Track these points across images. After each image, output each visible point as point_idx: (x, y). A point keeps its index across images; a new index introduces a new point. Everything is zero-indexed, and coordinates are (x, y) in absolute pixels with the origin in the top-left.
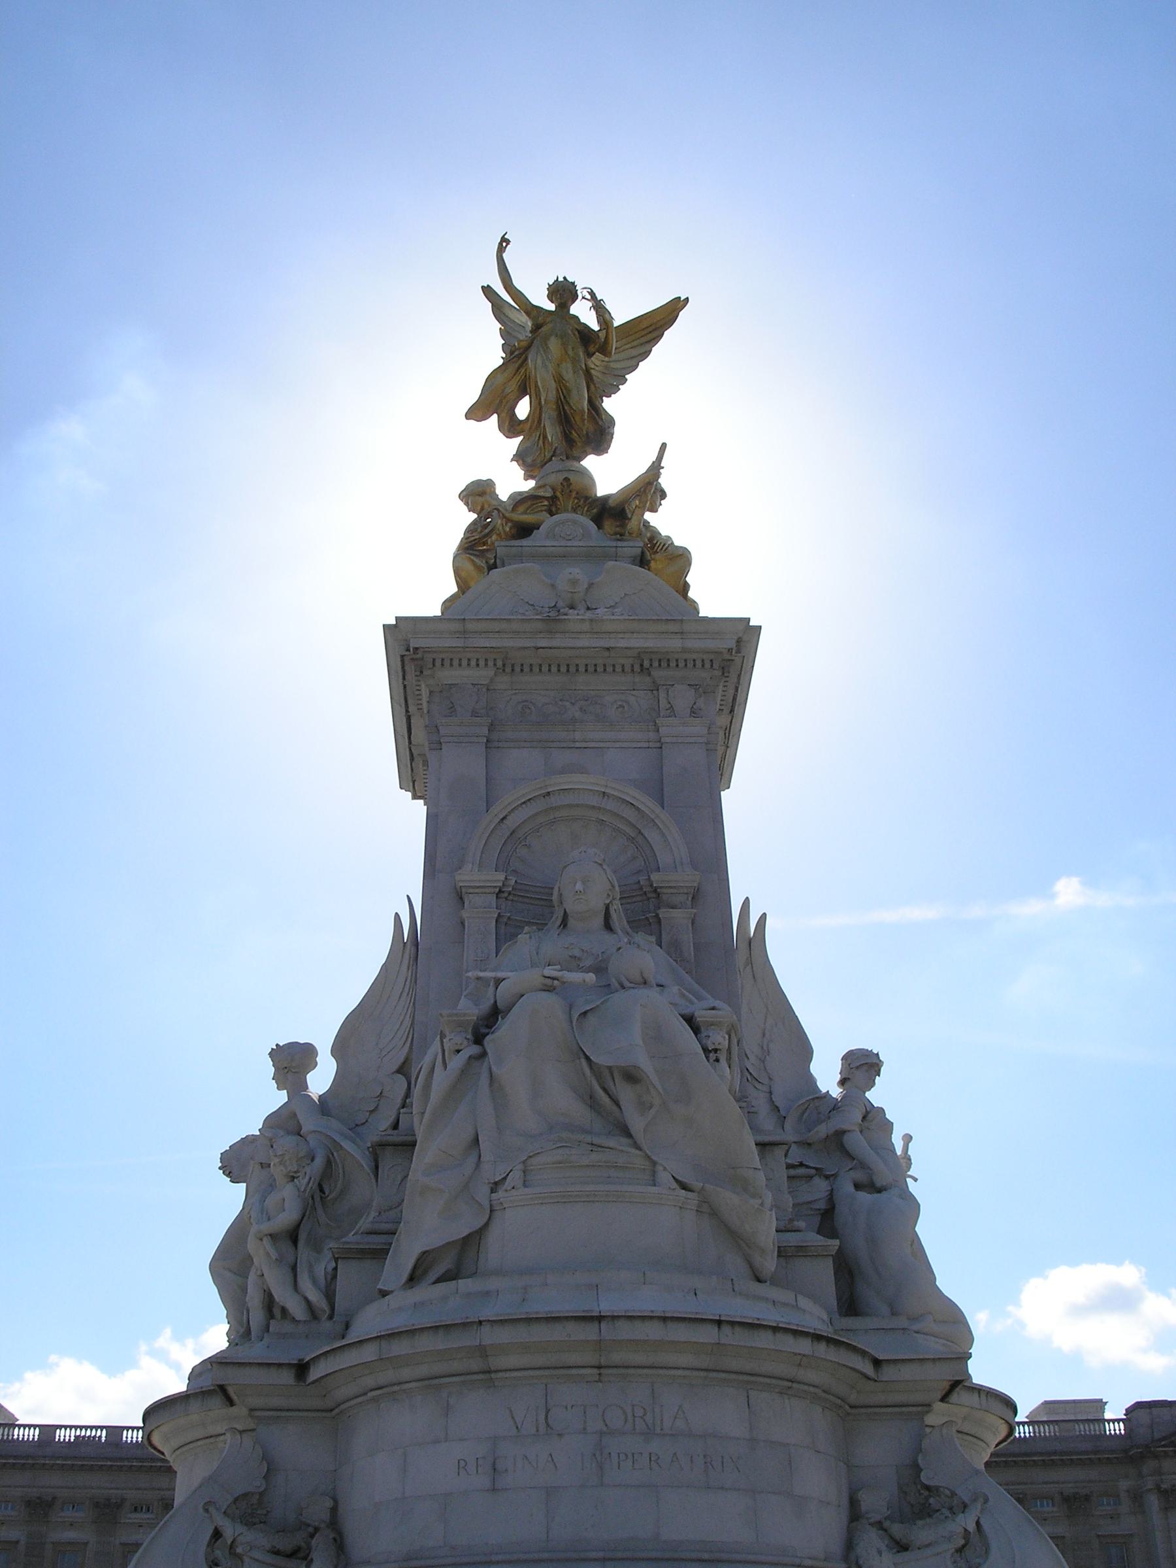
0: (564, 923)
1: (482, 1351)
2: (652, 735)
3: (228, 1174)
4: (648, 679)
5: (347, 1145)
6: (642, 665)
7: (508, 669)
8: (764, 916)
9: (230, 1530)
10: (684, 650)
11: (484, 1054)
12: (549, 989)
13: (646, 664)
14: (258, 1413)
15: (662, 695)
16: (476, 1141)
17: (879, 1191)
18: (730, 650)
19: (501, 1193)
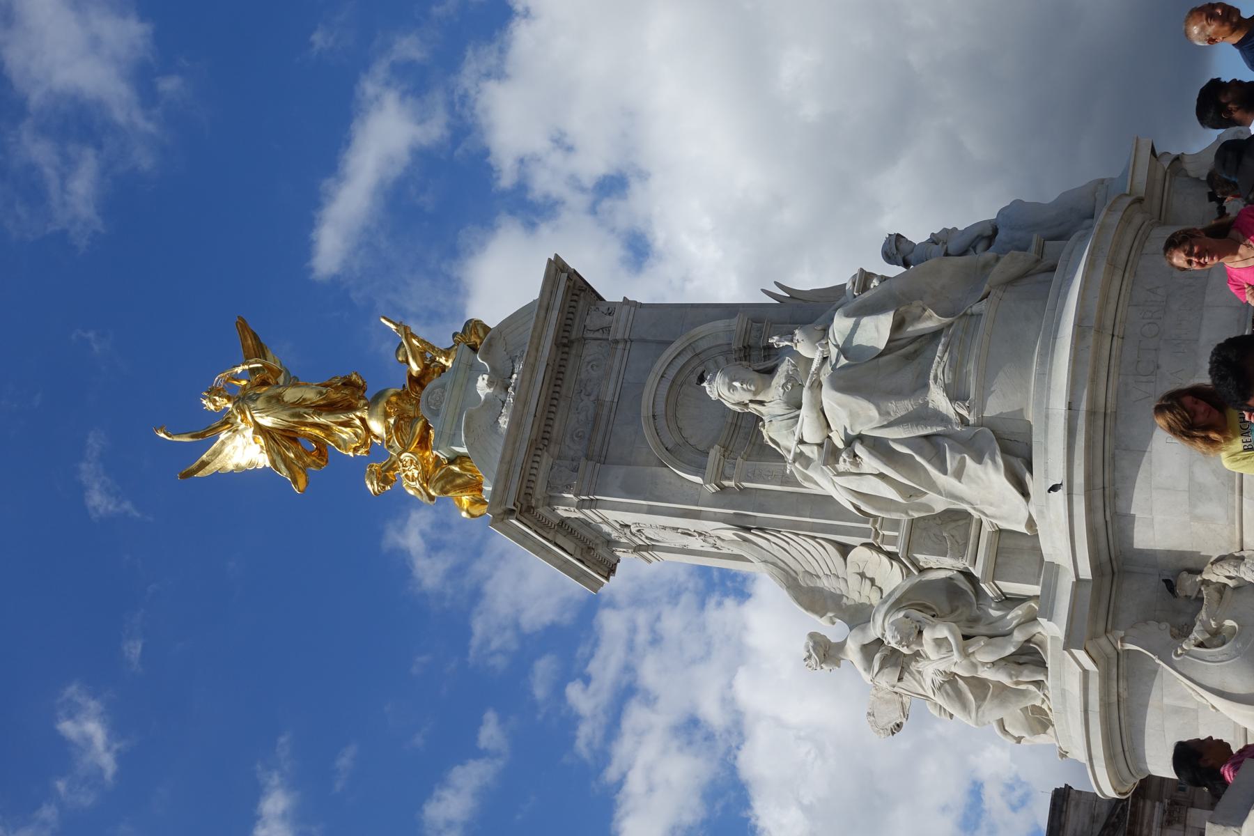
0: (762, 403)
1: (1092, 413)
2: (621, 346)
3: (899, 726)
4: (575, 345)
5: (897, 595)
6: (565, 345)
7: (546, 442)
8: (776, 283)
9: (1197, 635)
10: (561, 311)
11: (861, 438)
12: (820, 385)
13: (565, 341)
14: (1109, 627)
15: (590, 335)
16: (926, 437)
17: (995, 231)
18: (569, 278)
19: (972, 419)
